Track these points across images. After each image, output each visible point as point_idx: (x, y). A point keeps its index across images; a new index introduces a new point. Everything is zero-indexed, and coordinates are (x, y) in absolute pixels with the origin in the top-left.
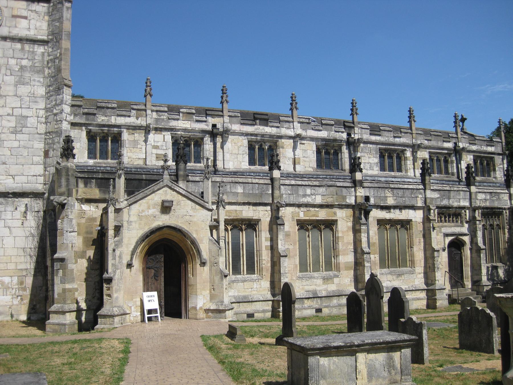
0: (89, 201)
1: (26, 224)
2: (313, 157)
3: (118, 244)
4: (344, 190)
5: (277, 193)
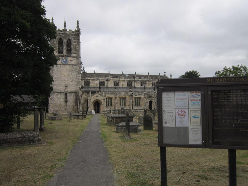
0: (85, 95)
2: (126, 84)
3: (90, 102)
5: (116, 93)
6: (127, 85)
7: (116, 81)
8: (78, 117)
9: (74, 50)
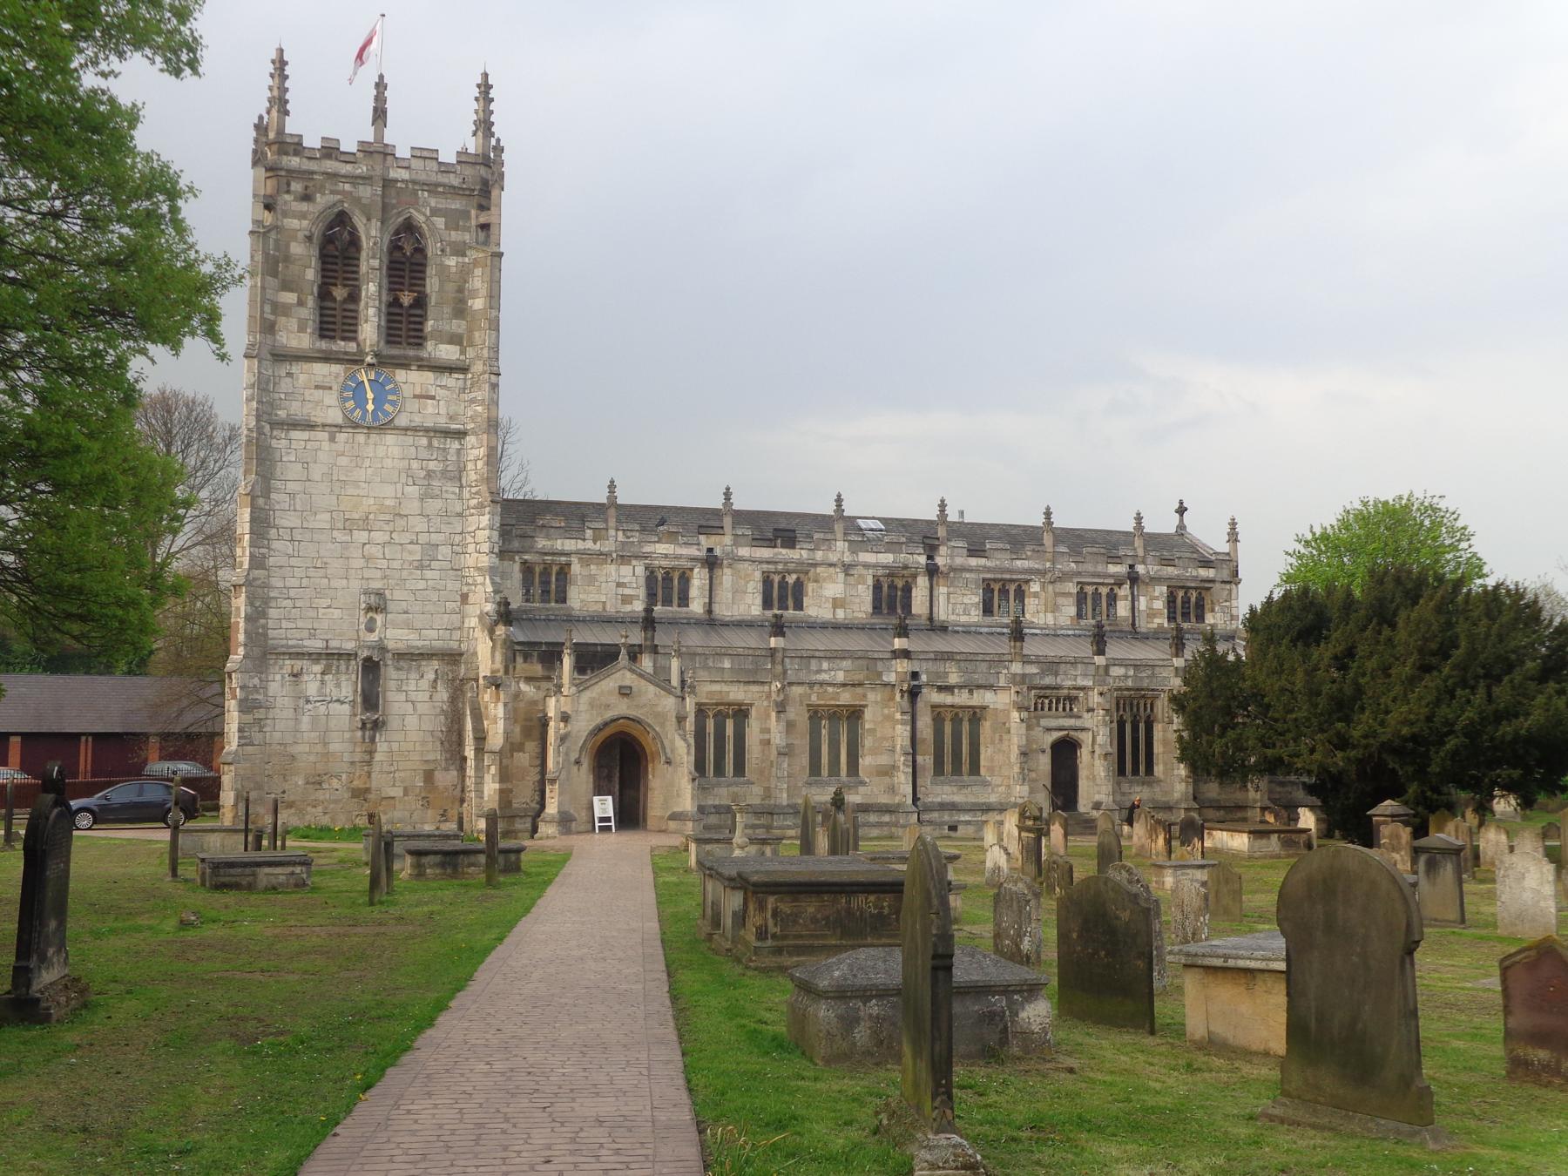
0: (529, 680)
1: (437, 697)
4: (880, 664)
6: (870, 610)
7: (780, 567)
8: (455, 867)
9: (447, 310)
